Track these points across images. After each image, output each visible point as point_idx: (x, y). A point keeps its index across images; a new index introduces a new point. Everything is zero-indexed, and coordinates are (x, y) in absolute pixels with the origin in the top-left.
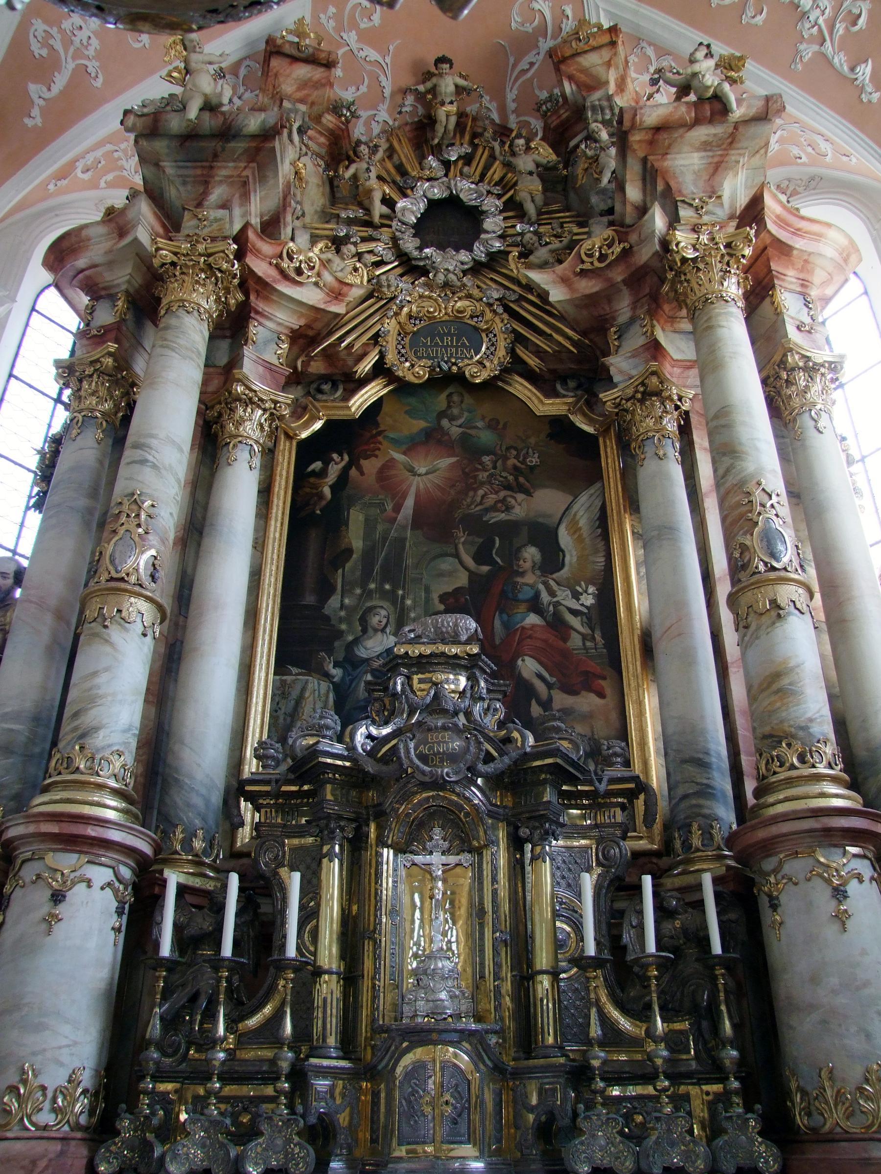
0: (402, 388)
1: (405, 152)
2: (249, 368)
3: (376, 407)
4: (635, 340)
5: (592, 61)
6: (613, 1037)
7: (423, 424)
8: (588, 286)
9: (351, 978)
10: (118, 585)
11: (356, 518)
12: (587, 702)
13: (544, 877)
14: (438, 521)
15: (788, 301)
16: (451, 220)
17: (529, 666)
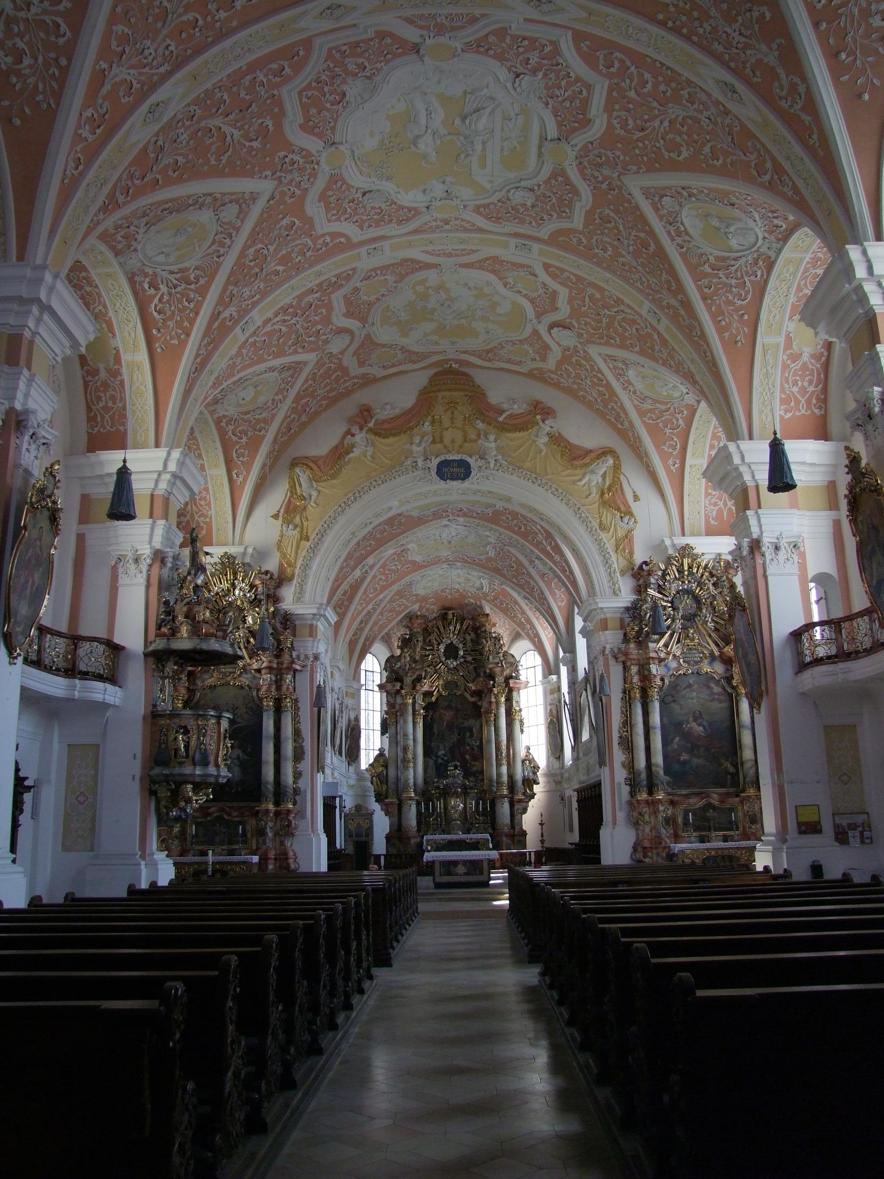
0: (441, 695)
1: (440, 623)
2: (417, 707)
3: (437, 699)
4: (487, 700)
5: (483, 619)
6: (476, 819)
7: (446, 703)
8: (479, 687)
9: (445, 814)
10: (409, 761)
11: (435, 726)
12: (477, 763)
13: (468, 801)
14: (450, 726)
15: (515, 694)
16: (451, 652)
17: (467, 757)
